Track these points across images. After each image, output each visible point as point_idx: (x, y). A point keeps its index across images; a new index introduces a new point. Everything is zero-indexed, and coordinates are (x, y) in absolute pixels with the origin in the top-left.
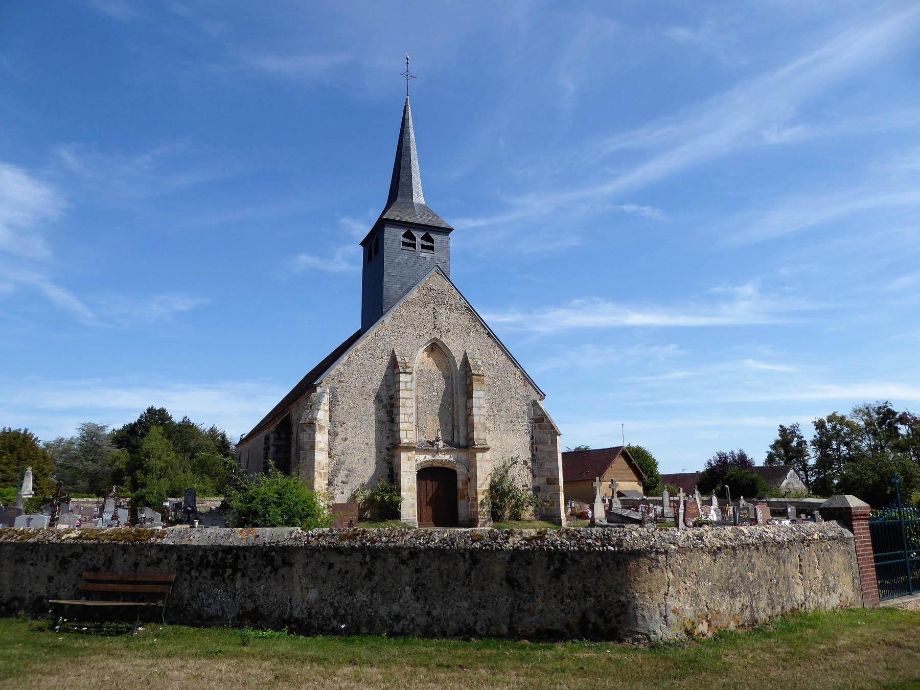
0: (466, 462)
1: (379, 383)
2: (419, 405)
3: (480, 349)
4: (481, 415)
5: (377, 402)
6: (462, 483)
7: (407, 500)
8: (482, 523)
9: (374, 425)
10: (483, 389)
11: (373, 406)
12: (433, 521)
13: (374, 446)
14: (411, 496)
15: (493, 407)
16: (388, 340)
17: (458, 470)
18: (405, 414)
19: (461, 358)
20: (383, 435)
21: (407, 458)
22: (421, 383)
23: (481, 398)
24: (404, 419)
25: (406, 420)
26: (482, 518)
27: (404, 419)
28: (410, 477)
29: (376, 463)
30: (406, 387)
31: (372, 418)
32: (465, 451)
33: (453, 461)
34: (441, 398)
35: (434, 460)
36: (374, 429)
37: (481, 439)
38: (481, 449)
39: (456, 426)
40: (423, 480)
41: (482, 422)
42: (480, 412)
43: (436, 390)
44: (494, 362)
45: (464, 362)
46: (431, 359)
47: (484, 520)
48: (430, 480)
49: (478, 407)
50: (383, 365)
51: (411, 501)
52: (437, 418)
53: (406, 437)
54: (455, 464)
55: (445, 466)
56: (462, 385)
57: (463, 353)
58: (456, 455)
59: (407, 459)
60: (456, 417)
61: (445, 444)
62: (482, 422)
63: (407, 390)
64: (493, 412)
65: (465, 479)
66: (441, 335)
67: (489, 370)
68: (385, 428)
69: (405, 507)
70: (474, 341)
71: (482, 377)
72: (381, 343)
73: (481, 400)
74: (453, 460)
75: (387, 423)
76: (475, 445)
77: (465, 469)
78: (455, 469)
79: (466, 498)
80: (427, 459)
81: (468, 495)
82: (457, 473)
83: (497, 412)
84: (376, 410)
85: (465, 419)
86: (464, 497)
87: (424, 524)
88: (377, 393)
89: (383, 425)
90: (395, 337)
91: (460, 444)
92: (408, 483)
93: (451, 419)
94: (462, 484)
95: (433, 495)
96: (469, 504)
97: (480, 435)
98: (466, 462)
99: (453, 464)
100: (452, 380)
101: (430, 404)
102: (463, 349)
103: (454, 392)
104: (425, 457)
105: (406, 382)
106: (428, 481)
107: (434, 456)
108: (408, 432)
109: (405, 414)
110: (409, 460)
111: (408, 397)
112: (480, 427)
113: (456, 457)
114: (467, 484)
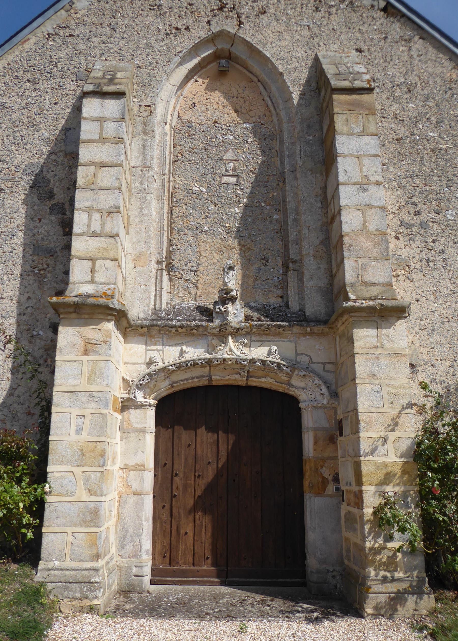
0: (328, 367)
1: (46, 149)
2: (176, 211)
3: (365, 48)
4: (370, 206)
5: (35, 199)
6: (315, 437)
7: (71, 494)
8: (383, 598)
9: (19, 261)
10: (372, 128)
11: (22, 210)
12: (213, 565)
13: (13, 321)
14: (87, 480)
15: (416, 200)
16: (81, 46)
17: (302, 396)
18: (90, 210)
19: (304, 75)
20: (46, 287)
21: (83, 343)
22: (187, 154)
23: (366, 156)
24: (89, 226)
25: (96, 226)
26: (385, 580)
27: (89, 226)
28: (87, 412)
29: (14, 371)
30: (101, 133)
31: (16, 240)
32: (322, 334)
33: (279, 365)
34: (248, 191)
35: (209, 362)
36: (18, 271)
37: (375, 284)
38: (371, 309)
39: (294, 262)
40: (185, 429)
41: (372, 228)
42: (363, 198)
43: (234, 169)
44: (412, 79)
45: (314, 84)
46: (217, 96)
47: (393, 588)
48: (209, 429)
49: (355, 184)
50: (62, 104)
51: (85, 497)
52: (234, 243)
53: (88, 278)
54: (290, 376)
55: (254, 382)
56: (308, 143)
57: (310, 62)
58: (292, 345)
59: (82, 349)
60: (292, 236)
61: (250, 312)
62: (372, 228)
63: (103, 141)
64: (418, 213)
65: (325, 424)
66: (241, 23)
67: (396, 99)
68: (54, 268)
69: (59, 521)
70: (345, 29)
71: (365, 98)
72: (63, 54)
73: (366, 161)
74: (279, 361)
75: (59, 254)
76: (347, 299)
77: (324, 390)
78: (292, 391)
79: (331, 488)
80: (187, 357)
81: (336, 479)
82: (301, 405)
83: (432, 215)
84: (30, 218)
85: (322, 237)
86: (324, 489)
87: (183, 573)
88: (38, 175)
89: (50, 261)
90: (104, 38)
91: (307, 314)
92: (79, 431)
93: (278, 246)
94: (315, 443)
95: (218, 476)
96: (343, 513)
97: (370, 270)
98: (328, 367)
99: (284, 377)
100: (282, 142)
101: (212, 207)
102: (309, 52)
103: (287, 167)
104: (182, 353)
105: (102, 120)
106: (202, 431)
107: (211, 349)
108: (98, 263)
109: (90, 210)
110: (86, 353)
111: (105, 159)
112: (366, 244)
113: (291, 354)
114: (332, 440)
